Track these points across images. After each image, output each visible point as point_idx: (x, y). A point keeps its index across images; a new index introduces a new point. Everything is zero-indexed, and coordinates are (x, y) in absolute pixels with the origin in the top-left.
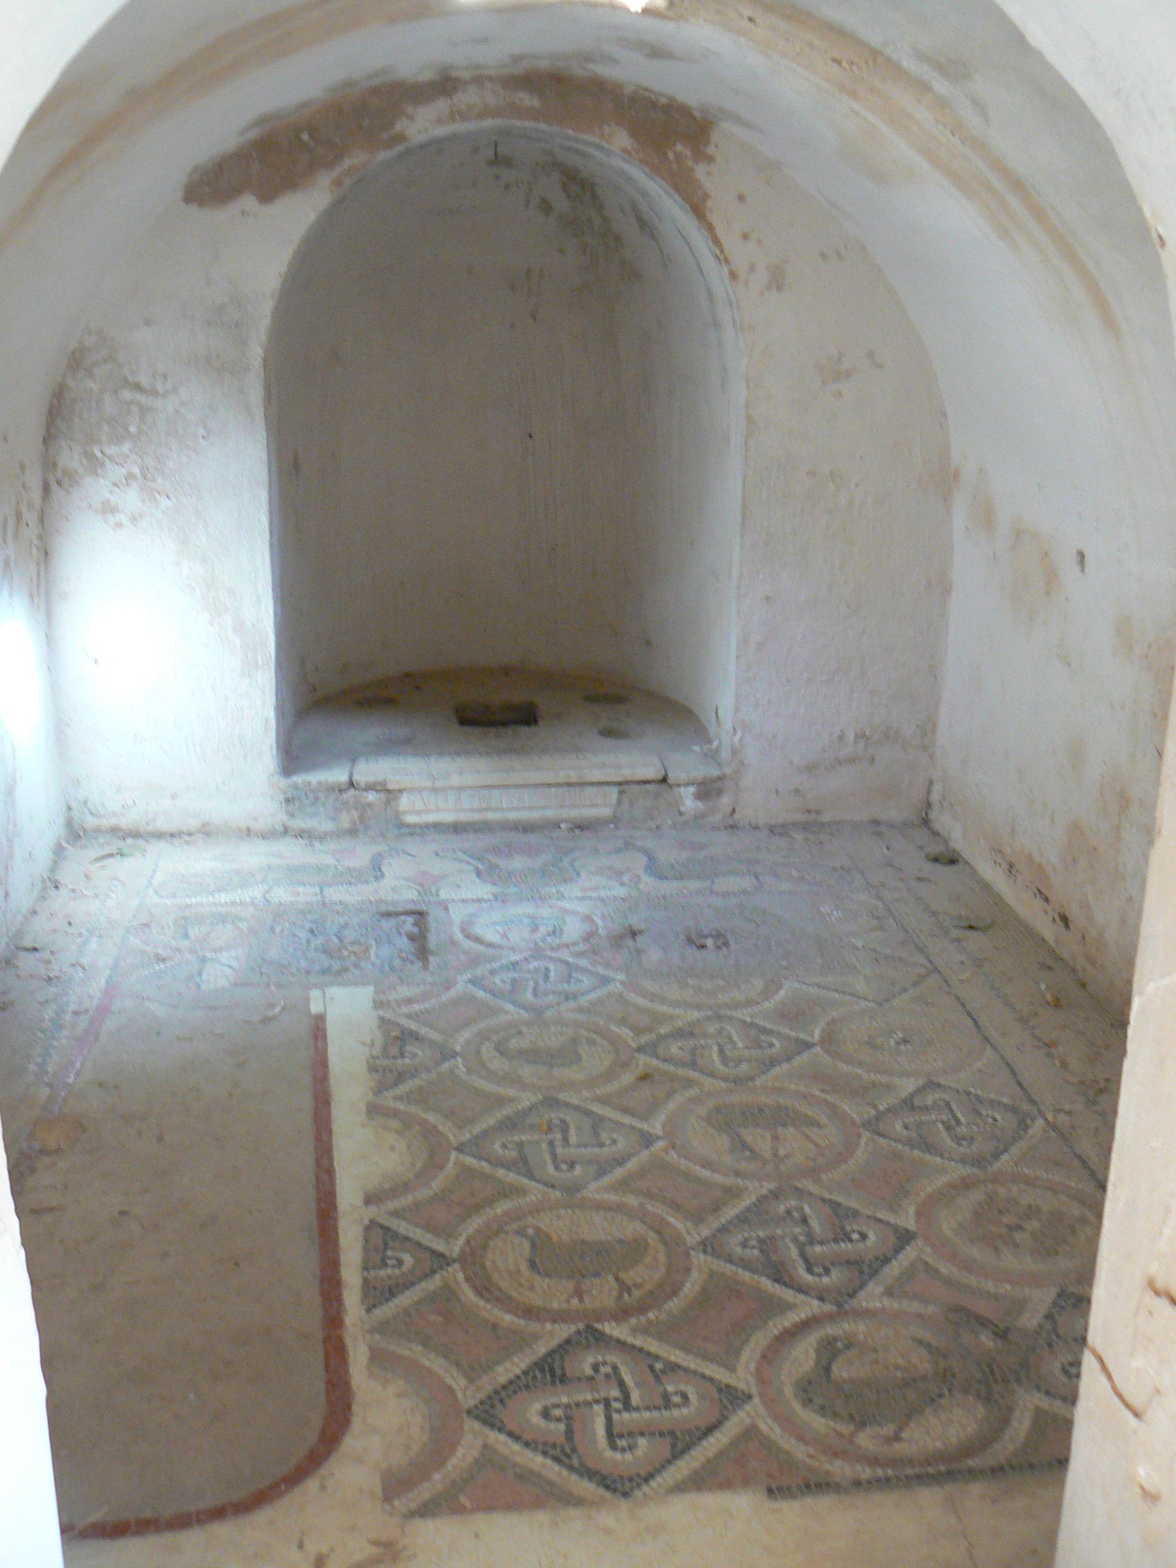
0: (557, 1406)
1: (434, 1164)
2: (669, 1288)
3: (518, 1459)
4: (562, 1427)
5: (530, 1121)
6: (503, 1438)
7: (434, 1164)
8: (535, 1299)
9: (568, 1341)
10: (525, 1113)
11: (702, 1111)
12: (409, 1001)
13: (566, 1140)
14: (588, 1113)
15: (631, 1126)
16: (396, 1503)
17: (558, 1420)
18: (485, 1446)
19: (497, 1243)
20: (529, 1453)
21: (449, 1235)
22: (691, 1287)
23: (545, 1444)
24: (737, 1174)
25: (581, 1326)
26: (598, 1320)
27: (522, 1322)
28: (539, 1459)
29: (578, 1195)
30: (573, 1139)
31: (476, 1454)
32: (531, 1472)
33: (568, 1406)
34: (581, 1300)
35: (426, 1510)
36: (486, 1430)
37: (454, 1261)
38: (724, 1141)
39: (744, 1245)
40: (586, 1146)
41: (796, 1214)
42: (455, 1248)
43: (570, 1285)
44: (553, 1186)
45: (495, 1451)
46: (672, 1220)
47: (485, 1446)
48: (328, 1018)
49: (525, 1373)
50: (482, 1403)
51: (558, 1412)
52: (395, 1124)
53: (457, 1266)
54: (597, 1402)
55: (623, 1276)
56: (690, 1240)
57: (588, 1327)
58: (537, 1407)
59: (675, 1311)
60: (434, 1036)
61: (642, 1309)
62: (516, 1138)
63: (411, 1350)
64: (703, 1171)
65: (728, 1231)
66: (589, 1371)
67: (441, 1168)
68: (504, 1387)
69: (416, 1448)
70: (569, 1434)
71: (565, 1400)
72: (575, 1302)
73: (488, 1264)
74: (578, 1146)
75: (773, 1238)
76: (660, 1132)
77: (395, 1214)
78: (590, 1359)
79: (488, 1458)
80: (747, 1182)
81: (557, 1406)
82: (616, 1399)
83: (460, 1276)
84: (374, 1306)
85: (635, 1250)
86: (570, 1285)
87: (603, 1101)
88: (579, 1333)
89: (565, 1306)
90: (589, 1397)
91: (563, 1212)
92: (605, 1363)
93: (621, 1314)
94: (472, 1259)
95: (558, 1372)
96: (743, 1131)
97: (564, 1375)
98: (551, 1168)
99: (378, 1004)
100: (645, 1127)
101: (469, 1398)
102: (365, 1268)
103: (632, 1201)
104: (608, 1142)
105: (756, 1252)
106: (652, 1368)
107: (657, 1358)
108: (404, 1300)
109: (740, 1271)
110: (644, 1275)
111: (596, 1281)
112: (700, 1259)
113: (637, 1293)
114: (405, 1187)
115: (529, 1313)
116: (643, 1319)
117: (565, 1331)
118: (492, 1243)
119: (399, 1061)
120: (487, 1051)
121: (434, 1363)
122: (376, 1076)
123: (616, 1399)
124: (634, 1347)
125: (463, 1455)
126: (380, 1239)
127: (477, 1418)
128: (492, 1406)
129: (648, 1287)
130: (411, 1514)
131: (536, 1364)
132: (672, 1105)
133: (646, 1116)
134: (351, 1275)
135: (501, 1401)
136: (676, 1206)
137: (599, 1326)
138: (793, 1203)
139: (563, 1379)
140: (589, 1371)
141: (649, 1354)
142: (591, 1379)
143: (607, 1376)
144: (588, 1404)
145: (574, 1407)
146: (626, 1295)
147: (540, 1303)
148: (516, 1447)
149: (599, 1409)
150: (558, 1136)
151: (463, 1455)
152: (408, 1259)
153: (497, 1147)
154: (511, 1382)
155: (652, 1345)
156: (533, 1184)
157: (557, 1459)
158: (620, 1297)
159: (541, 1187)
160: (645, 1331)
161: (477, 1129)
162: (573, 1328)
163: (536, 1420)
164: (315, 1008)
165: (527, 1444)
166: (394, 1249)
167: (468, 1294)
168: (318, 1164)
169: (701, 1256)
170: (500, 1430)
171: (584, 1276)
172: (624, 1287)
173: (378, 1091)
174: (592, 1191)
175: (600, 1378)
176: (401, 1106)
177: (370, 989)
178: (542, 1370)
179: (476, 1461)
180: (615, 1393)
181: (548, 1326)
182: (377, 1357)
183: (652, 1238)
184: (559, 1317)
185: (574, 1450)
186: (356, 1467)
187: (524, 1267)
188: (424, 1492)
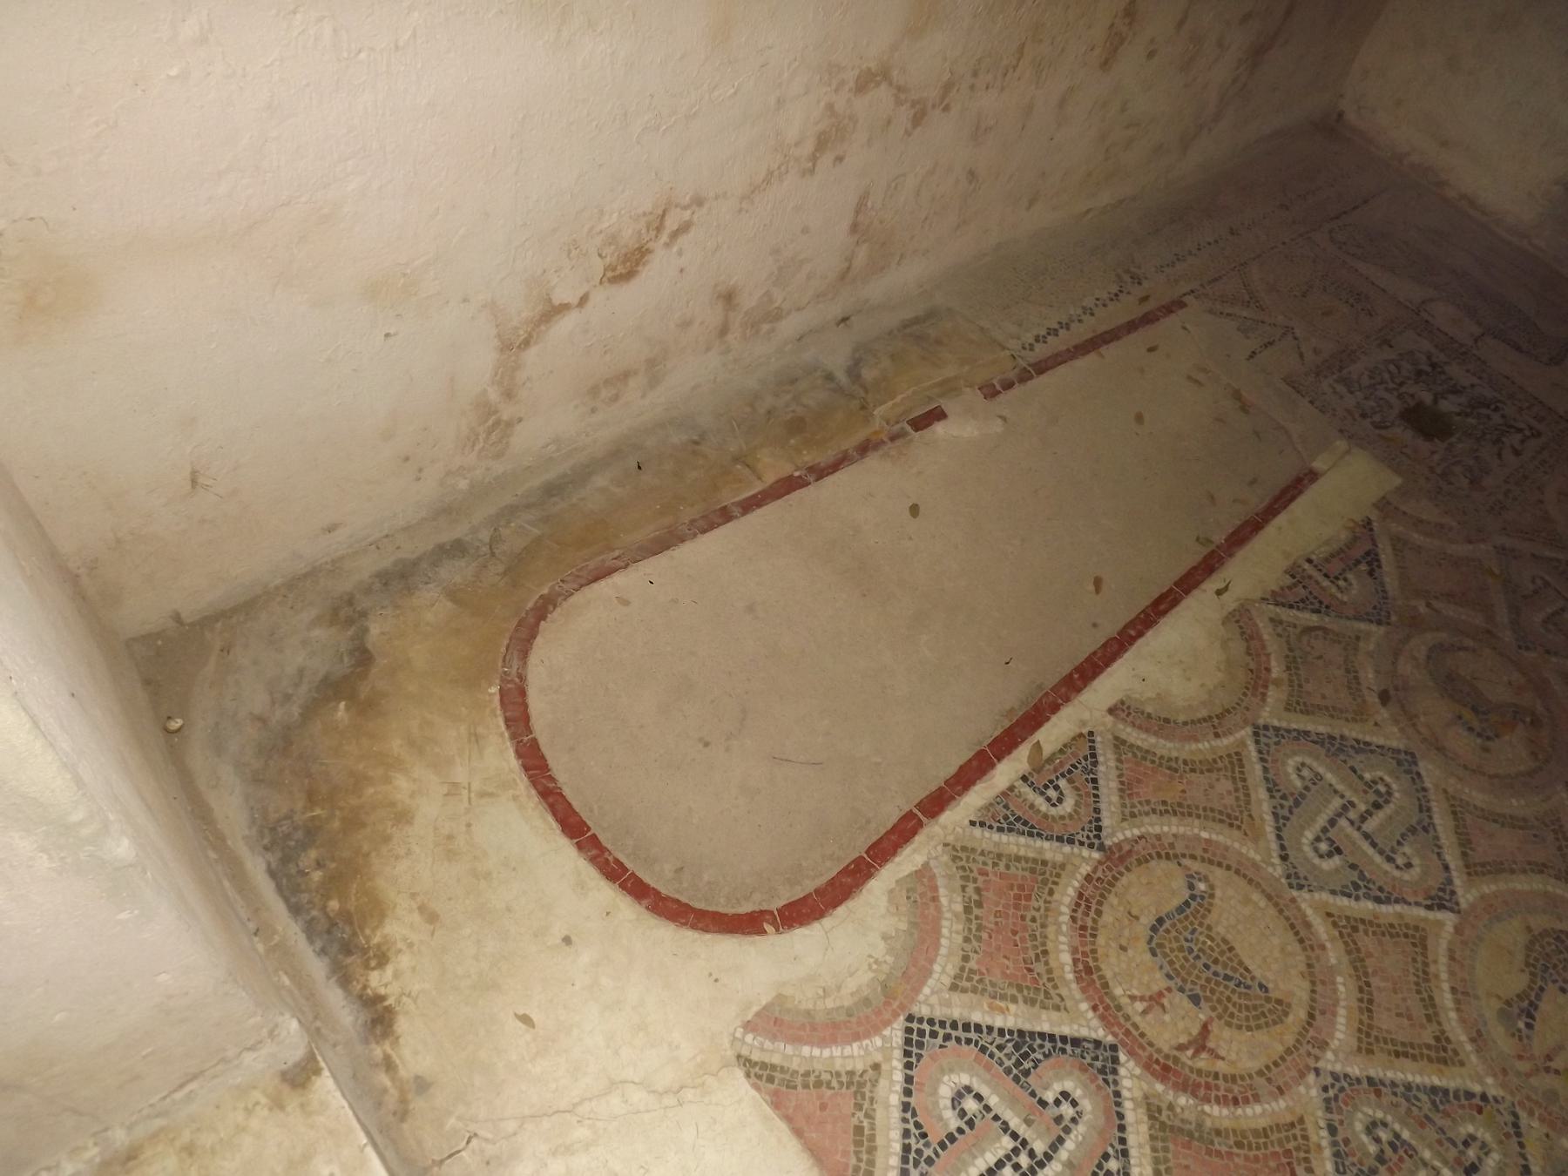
0: (979, 1097)
1: (1216, 723)
2: (1237, 1092)
3: (880, 1114)
4: (954, 1123)
5: (1357, 760)
6: (899, 1076)
7: (1216, 723)
8: (1111, 965)
9: (1076, 1042)
10: (1363, 747)
11: (1540, 922)
12: (1418, 523)
13: (1363, 819)
14: (1425, 809)
15: (1446, 868)
16: (749, 1038)
17: (963, 1113)
18: (876, 1067)
19: (1159, 867)
20: (896, 1114)
21: (1129, 816)
22: (1254, 1115)
23: (918, 1125)
24: (1478, 1038)
25: (1110, 1039)
26: (1131, 1053)
27: (1070, 976)
28: (896, 1135)
29: (1295, 893)
30: (1369, 826)
31: (860, 1067)
32: (872, 1138)
33: (987, 1108)
34: (1145, 1012)
35: (760, 1073)
36: (898, 1053)
37: (1101, 848)
38: (1517, 982)
39: (1371, 1127)
40: (1374, 845)
41: (1471, 1153)
42: (1117, 832)
43: (1159, 983)
44: (1284, 858)
45: (875, 1083)
46: (1341, 1020)
47: (876, 1067)
48: (1321, 482)
49: (1001, 1032)
50: (931, 1022)
51: (970, 1105)
52: (1238, 647)
53: (1096, 855)
54: (1015, 1136)
55: (1215, 1028)
56: (1330, 1062)
57: (1114, 1048)
58: (965, 1079)
59: (1208, 1123)
60: (1391, 581)
61: (1185, 1087)
62: (1321, 770)
63: (951, 901)
64: (1448, 996)
65: (1378, 1093)
66: (1050, 1097)
67: (1217, 735)
68: (966, 1027)
69: (830, 1004)
70: (951, 1138)
71: (993, 1101)
72: (1139, 1006)
73: (1124, 880)
74: (1366, 836)
75: (1411, 1151)
76: (1464, 905)
77: (1119, 743)
78: (1068, 1085)
79: (859, 1085)
80: (1473, 1058)
81: (979, 1097)
82: (1032, 1154)
83: (1086, 869)
84: (982, 824)
85: (1261, 1008)
86: (1159, 983)
87: (1457, 810)
88: (1097, 1043)
89: (1125, 1001)
90: (1015, 1123)
91: (1256, 896)
92: (1074, 1103)
93: (1163, 1069)
94: (1118, 859)
95: (1027, 1065)
96: (1551, 989)
97: (1027, 1073)
98: (1309, 835)
99: (1383, 505)
100: (1458, 882)
101: (934, 999)
102: (1024, 778)
103: (1334, 955)
104: (1400, 861)
105: (1373, 1149)
106: (1106, 1157)
107: (1125, 1153)
108: (1015, 844)
109: (1327, 1153)
110: (1239, 1051)
111: (1187, 1004)
112: (1310, 1092)
113: (1203, 1062)
114: (1163, 725)
115: (1087, 971)
116: (1170, 1096)
117: (1089, 1027)
118: (1153, 863)
119: (1326, 583)
120: (1420, 645)
121: (951, 934)
122: (1289, 581)
123: (1032, 1154)
124: (1121, 1116)
125: (850, 1056)
126: (1080, 759)
127: (909, 1030)
128: (934, 1035)
129: (1221, 1066)
130: (745, 1062)
131: (1021, 1033)
132: (1521, 884)
133: (1474, 870)
134: (1005, 773)
135: (947, 1037)
136: (1367, 1004)
137: (1122, 1057)
138: (1488, 1137)
139: (1020, 1076)
140: (1050, 1097)
141: (1123, 1141)
142: (1043, 1103)
143: (1059, 1119)
144: (1005, 1127)
145: (992, 1115)
146: (1190, 1053)
147: (1109, 974)
148: (895, 1099)
149: (1007, 1143)
150: (1362, 807)
151: (850, 1056)
152: (1068, 806)
153: (1291, 763)
154: (978, 1028)
155: (1138, 1135)
156: (1272, 837)
157: (906, 1149)
158: (1181, 1048)
159: (1274, 846)
160: (1153, 1111)
161: (1299, 723)
162: (1100, 1033)
163: (946, 1092)
164: (1318, 464)
165: (906, 1107)
166: (1070, 781)
167: (1067, 894)
168: (1122, 632)
169: (1314, 1092)
170: (908, 1066)
171: (1181, 990)
172: (1200, 1043)
173: (1276, 598)
174: (1308, 903)
175: (1053, 1111)
176: (1267, 632)
177: (1398, 481)
178: (1017, 1047)
179: (851, 1073)
180: (1039, 1147)
181: (1084, 1006)
182: (923, 874)
183: (1299, 1014)
184: (1107, 1010)
185: (929, 1161)
186: (765, 967)
187: (1147, 920)
188: (780, 1053)
